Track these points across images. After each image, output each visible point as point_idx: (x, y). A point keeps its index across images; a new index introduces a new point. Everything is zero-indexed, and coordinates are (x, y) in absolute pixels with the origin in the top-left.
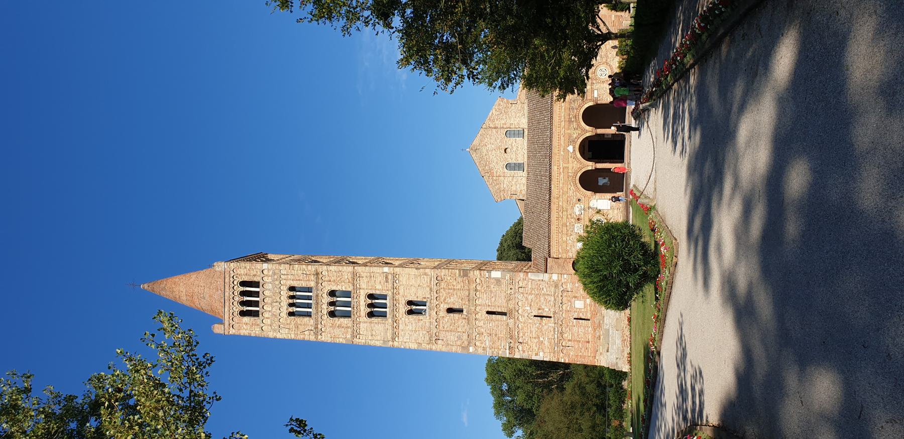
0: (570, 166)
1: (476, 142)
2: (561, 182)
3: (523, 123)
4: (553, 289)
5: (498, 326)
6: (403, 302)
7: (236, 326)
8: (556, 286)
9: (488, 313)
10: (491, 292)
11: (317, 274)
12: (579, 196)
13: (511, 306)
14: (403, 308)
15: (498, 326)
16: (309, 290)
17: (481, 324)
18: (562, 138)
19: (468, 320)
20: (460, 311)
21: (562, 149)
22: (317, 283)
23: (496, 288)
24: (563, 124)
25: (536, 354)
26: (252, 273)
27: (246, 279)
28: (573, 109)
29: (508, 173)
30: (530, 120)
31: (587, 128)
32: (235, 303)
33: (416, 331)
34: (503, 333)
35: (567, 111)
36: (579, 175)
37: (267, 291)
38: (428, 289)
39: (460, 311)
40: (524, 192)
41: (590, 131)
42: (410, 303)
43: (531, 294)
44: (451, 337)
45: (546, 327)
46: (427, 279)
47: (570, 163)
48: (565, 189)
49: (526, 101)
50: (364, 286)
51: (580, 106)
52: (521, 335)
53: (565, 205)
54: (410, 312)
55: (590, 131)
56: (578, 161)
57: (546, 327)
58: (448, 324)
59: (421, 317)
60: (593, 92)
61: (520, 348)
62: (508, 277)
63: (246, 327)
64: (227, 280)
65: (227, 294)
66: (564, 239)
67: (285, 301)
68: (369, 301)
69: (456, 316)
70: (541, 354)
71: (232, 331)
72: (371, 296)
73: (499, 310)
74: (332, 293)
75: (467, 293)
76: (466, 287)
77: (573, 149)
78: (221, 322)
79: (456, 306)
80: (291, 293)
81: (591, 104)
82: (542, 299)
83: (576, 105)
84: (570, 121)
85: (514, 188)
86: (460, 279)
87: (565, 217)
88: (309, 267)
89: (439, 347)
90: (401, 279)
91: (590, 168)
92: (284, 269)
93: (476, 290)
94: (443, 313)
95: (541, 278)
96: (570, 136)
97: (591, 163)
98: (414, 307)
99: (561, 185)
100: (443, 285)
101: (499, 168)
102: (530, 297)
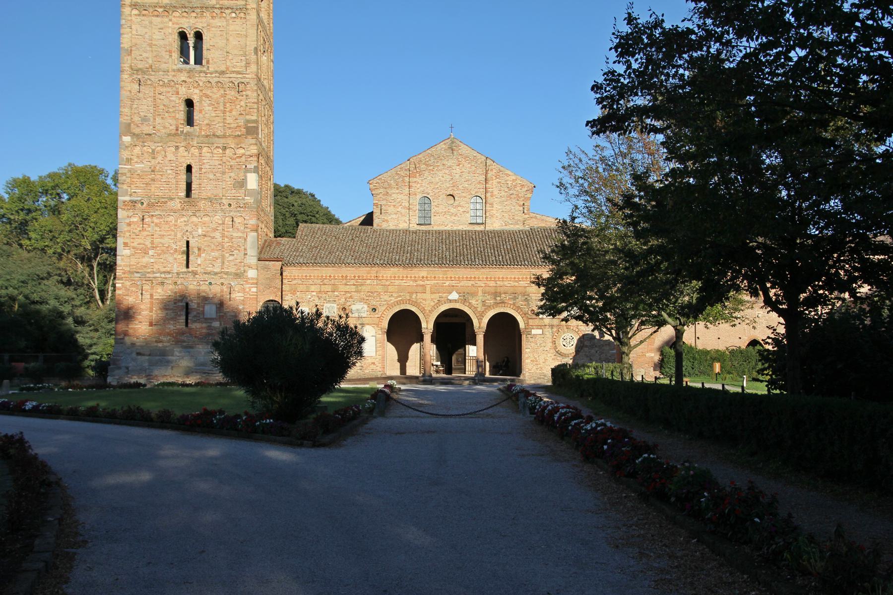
0: (428, 296)
1: (464, 149)
2: (403, 283)
3: (495, 224)
4: (233, 270)
5: (168, 183)
6: (200, 25)
8: (238, 275)
9: (189, 168)
10: (224, 173)
12: (381, 309)
13: (202, 204)
14: (190, 25)
15: (168, 183)
17: (170, 156)
18: (470, 283)
19: (176, 134)
20: (190, 121)
21: (453, 283)
23: (230, 182)
24: (492, 284)
25: (126, 244)
28: (515, 298)
29: (416, 200)
30: (498, 234)
31: (485, 321)
33: (151, 45)
34: (157, 190)
35: (512, 290)
36: (414, 309)
38: (223, 68)
39: (190, 121)
40: (384, 226)
41: (480, 324)
42: (199, 36)
43: (223, 236)
44: (148, 104)
45: (171, 259)
46: (240, 66)
47: (432, 293)
48: (391, 289)
49: (527, 228)
51: (518, 309)
52: (156, 220)
53: (367, 288)
54: (183, 36)
55: (480, 324)
56: (434, 308)
57: (171, 259)
58: (166, 102)
59: (176, 55)
60: (539, 327)
62: (249, 200)
66: (313, 288)
69: (182, 115)
70: (127, 252)
73: (194, 186)
75: (219, 133)
76: (229, 132)
77: (453, 300)
79: (197, 116)
81: (522, 325)
82: (216, 254)
83: (520, 302)
84: (496, 294)
85: (391, 209)
86: (241, 122)
87: (347, 288)
89: (128, 85)
90: (238, 21)
91: (424, 325)
93: (225, 149)
94: (184, 92)
95: (249, 252)
96: (474, 294)
97: (431, 326)
98: (191, 42)
99: (397, 282)
100: (232, 94)
101: (422, 185)
102: (217, 235)
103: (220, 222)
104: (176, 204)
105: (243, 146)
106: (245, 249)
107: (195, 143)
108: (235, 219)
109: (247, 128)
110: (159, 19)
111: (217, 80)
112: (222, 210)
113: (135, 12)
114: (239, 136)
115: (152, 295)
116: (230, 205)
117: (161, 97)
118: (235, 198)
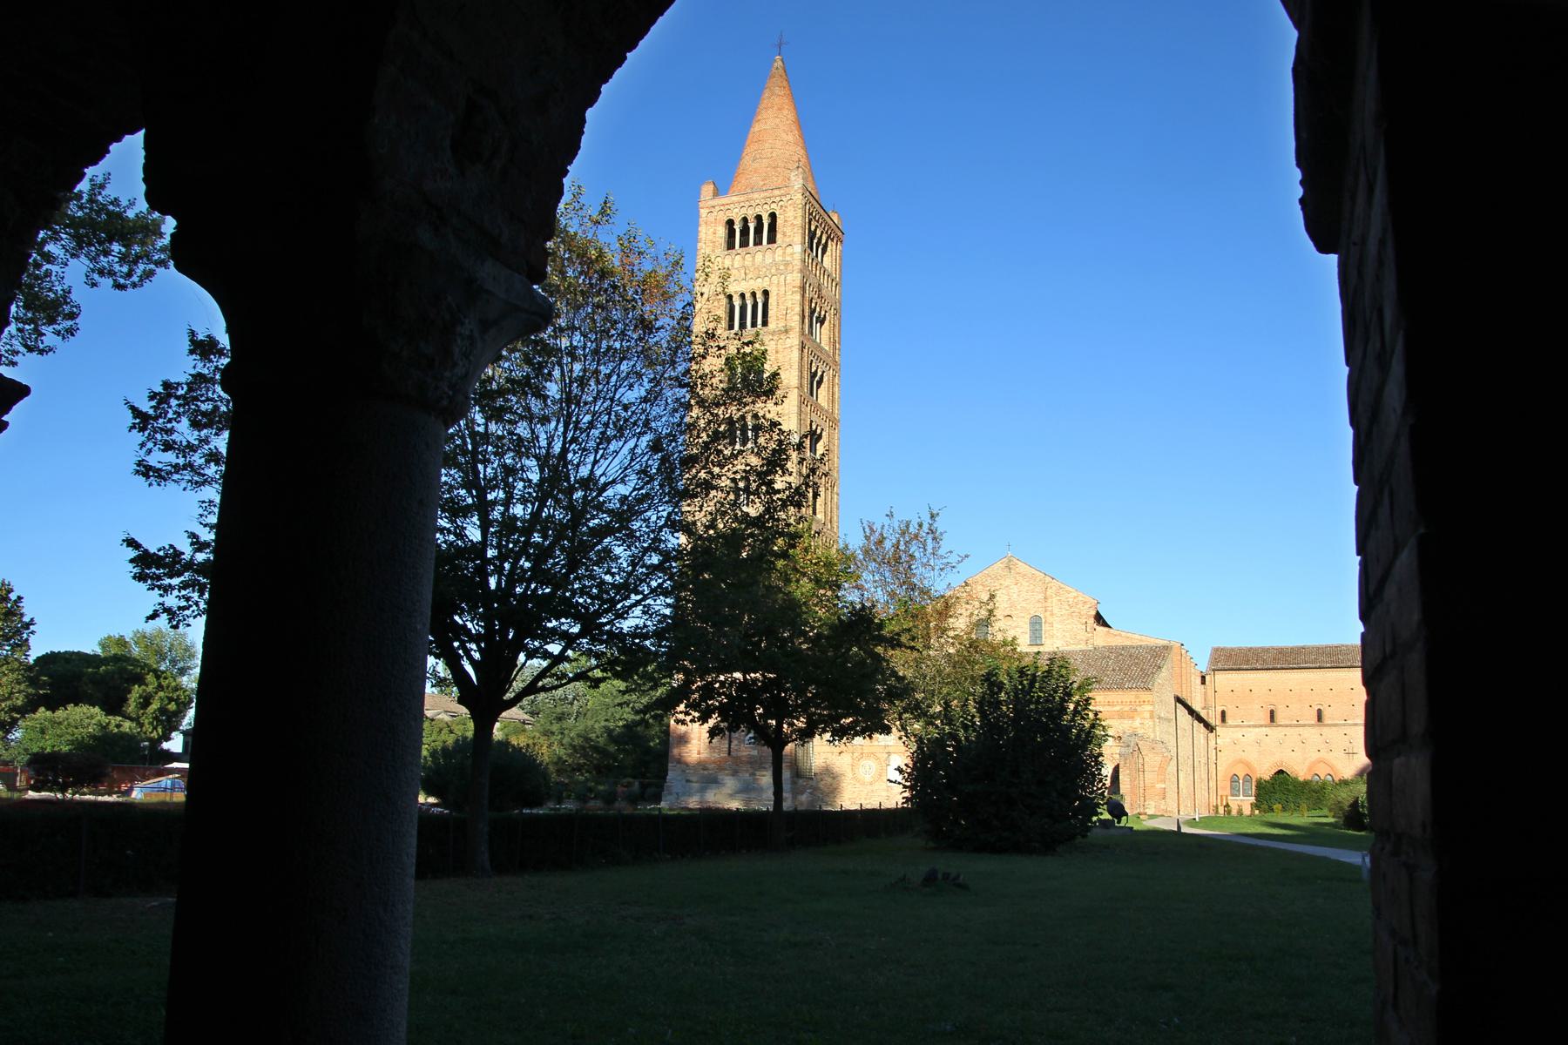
1: (1022, 567)
7: (711, 217)
11: (786, 331)
16: (765, 323)
22: (773, 333)
26: (788, 230)
27: (779, 222)
32: (744, 211)
37: (760, 256)
49: (1090, 647)
63: (711, 234)
64: (777, 192)
65: (756, 195)
67: (746, 287)
71: (703, 212)
78: (716, 194)
88: (797, 318)
92: (795, 278)
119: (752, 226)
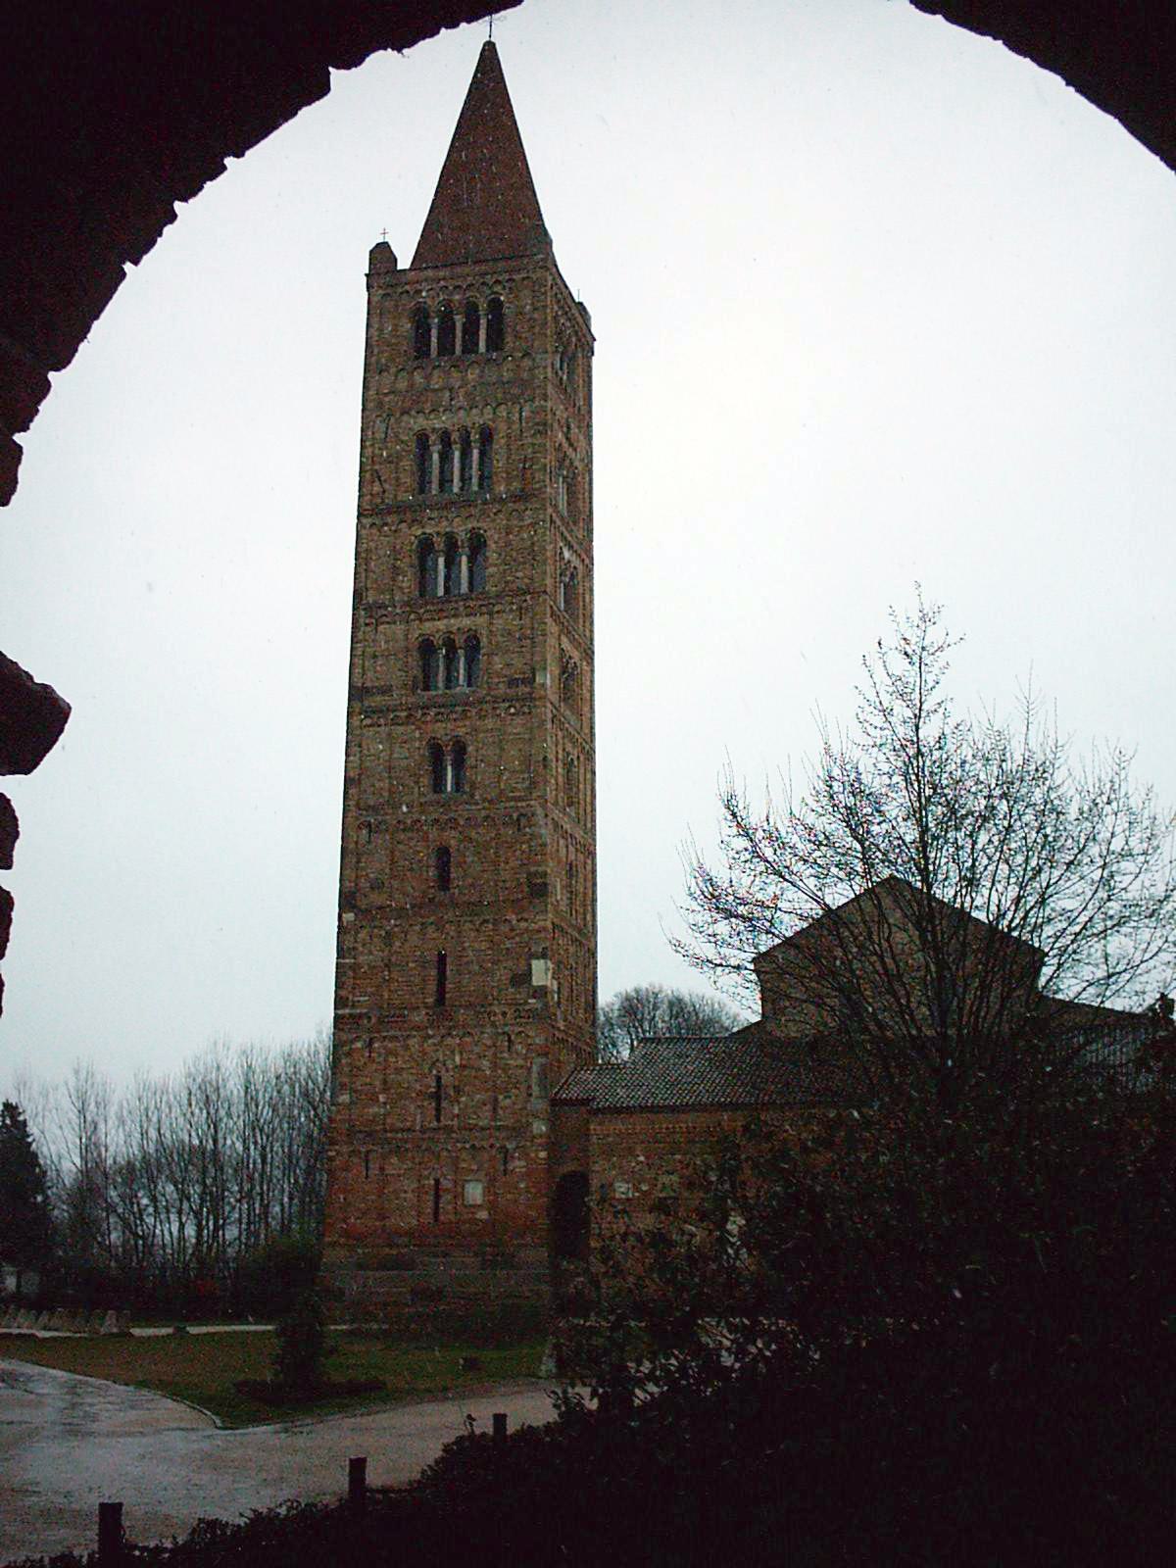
4: (510, 1122)
9: (442, 960)
13: (462, 1015)
14: (442, 730)
17: (414, 939)
20: (444, 881)
42: (460, 749)
43: (495, 1066)
50: (499, 622)
54: (436, 753)
59: (425, 781)
61: (359, 1045)
64: (501, 265)
68: (460, 640)
72: (473, 645)
74: (477, 544)
80: (475, 436)
90: (518, 720)
103: (489, 1043)
104: (419, 1017)
105: (525, 915)
106: (530, 1087)
107: (449, 916)
108: (513, 1037)
109: (531, 885)
110: (401, 729)
111: (483, 813)
112: (493, 1024)
113: (368, 721)
114: (518, 900)
115: (382, 1169)
116: (504, 1014)
117: (400, 846)
118: (514, 1003)
119: (459, 320)
